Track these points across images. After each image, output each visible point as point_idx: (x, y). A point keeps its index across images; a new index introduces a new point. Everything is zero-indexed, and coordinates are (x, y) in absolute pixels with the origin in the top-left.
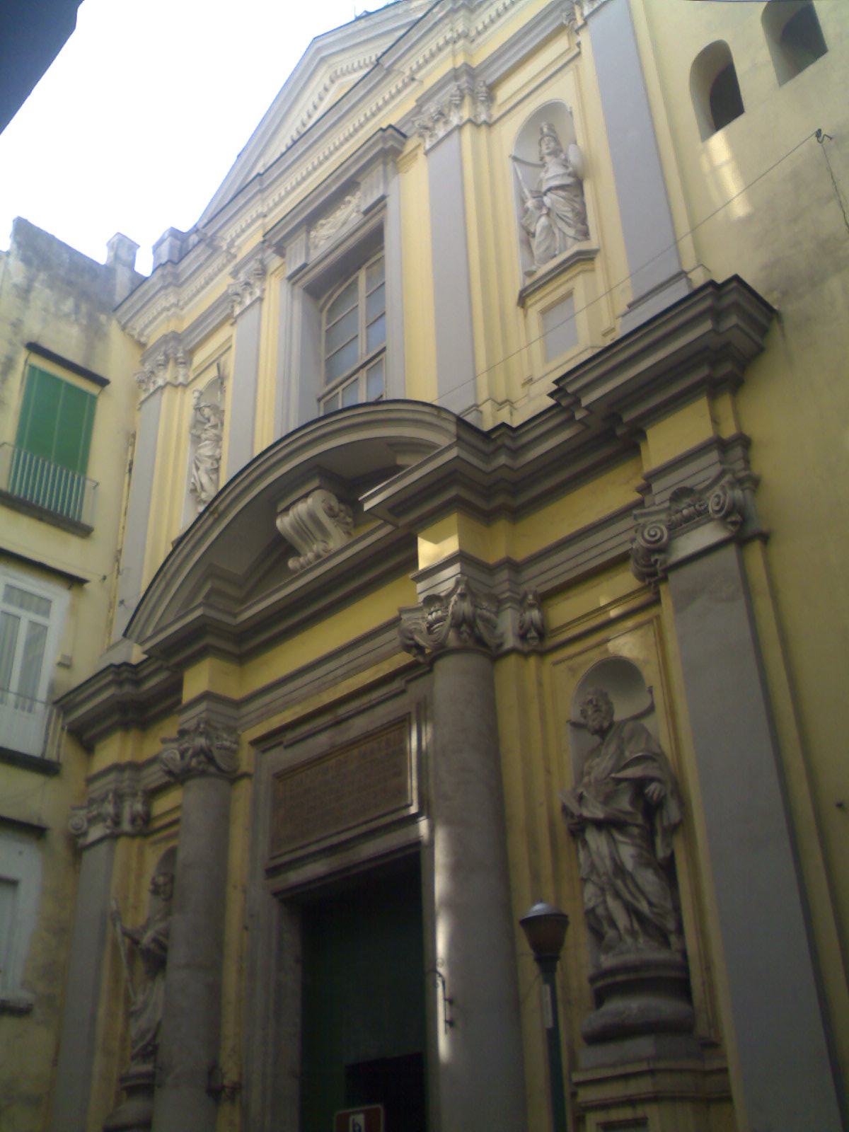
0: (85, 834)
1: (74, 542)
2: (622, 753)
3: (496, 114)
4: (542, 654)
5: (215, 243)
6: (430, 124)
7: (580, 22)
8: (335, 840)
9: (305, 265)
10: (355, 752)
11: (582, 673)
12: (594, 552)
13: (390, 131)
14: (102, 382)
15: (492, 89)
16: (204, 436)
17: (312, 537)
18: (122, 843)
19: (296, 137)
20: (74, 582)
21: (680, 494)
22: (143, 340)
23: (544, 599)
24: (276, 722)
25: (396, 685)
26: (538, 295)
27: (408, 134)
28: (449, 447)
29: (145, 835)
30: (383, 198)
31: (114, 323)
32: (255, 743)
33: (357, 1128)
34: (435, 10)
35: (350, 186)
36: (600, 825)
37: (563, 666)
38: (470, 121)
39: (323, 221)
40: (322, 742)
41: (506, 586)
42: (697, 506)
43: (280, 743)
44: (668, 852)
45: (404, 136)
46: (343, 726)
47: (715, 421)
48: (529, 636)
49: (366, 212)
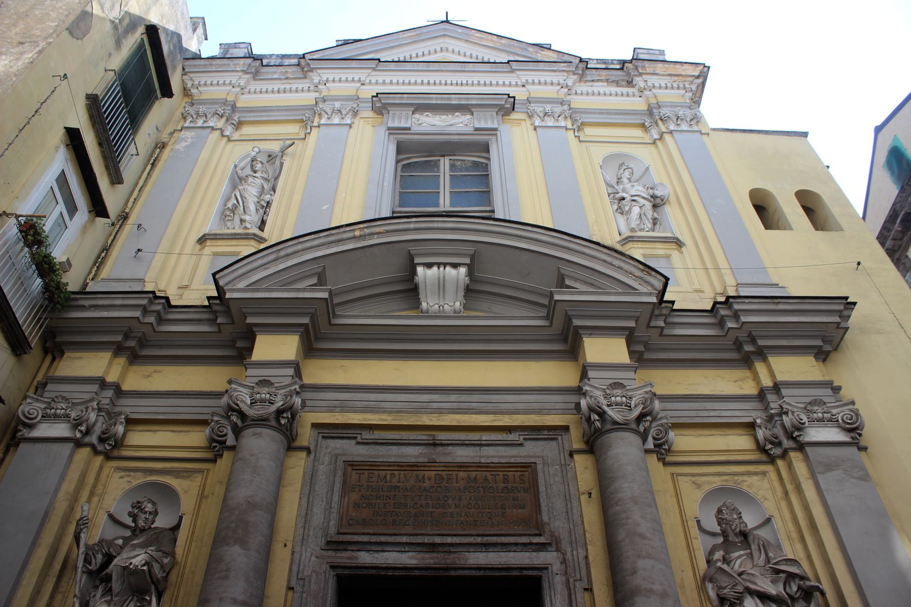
0: (31, 427)
8: (438, 540)
11: (707, 488)
12: (706, 414)
13: (512, 100)
17: (441, 295)
18: (85, 452)
19: (402, 59)
25: (512, 437)
28: (650, 294)
32: (315, 426)
34: (562, 64)
37: (686, 479)
40: (412, 453)
43: (356, 438)
46: (440, 449)
49: (477, 129)
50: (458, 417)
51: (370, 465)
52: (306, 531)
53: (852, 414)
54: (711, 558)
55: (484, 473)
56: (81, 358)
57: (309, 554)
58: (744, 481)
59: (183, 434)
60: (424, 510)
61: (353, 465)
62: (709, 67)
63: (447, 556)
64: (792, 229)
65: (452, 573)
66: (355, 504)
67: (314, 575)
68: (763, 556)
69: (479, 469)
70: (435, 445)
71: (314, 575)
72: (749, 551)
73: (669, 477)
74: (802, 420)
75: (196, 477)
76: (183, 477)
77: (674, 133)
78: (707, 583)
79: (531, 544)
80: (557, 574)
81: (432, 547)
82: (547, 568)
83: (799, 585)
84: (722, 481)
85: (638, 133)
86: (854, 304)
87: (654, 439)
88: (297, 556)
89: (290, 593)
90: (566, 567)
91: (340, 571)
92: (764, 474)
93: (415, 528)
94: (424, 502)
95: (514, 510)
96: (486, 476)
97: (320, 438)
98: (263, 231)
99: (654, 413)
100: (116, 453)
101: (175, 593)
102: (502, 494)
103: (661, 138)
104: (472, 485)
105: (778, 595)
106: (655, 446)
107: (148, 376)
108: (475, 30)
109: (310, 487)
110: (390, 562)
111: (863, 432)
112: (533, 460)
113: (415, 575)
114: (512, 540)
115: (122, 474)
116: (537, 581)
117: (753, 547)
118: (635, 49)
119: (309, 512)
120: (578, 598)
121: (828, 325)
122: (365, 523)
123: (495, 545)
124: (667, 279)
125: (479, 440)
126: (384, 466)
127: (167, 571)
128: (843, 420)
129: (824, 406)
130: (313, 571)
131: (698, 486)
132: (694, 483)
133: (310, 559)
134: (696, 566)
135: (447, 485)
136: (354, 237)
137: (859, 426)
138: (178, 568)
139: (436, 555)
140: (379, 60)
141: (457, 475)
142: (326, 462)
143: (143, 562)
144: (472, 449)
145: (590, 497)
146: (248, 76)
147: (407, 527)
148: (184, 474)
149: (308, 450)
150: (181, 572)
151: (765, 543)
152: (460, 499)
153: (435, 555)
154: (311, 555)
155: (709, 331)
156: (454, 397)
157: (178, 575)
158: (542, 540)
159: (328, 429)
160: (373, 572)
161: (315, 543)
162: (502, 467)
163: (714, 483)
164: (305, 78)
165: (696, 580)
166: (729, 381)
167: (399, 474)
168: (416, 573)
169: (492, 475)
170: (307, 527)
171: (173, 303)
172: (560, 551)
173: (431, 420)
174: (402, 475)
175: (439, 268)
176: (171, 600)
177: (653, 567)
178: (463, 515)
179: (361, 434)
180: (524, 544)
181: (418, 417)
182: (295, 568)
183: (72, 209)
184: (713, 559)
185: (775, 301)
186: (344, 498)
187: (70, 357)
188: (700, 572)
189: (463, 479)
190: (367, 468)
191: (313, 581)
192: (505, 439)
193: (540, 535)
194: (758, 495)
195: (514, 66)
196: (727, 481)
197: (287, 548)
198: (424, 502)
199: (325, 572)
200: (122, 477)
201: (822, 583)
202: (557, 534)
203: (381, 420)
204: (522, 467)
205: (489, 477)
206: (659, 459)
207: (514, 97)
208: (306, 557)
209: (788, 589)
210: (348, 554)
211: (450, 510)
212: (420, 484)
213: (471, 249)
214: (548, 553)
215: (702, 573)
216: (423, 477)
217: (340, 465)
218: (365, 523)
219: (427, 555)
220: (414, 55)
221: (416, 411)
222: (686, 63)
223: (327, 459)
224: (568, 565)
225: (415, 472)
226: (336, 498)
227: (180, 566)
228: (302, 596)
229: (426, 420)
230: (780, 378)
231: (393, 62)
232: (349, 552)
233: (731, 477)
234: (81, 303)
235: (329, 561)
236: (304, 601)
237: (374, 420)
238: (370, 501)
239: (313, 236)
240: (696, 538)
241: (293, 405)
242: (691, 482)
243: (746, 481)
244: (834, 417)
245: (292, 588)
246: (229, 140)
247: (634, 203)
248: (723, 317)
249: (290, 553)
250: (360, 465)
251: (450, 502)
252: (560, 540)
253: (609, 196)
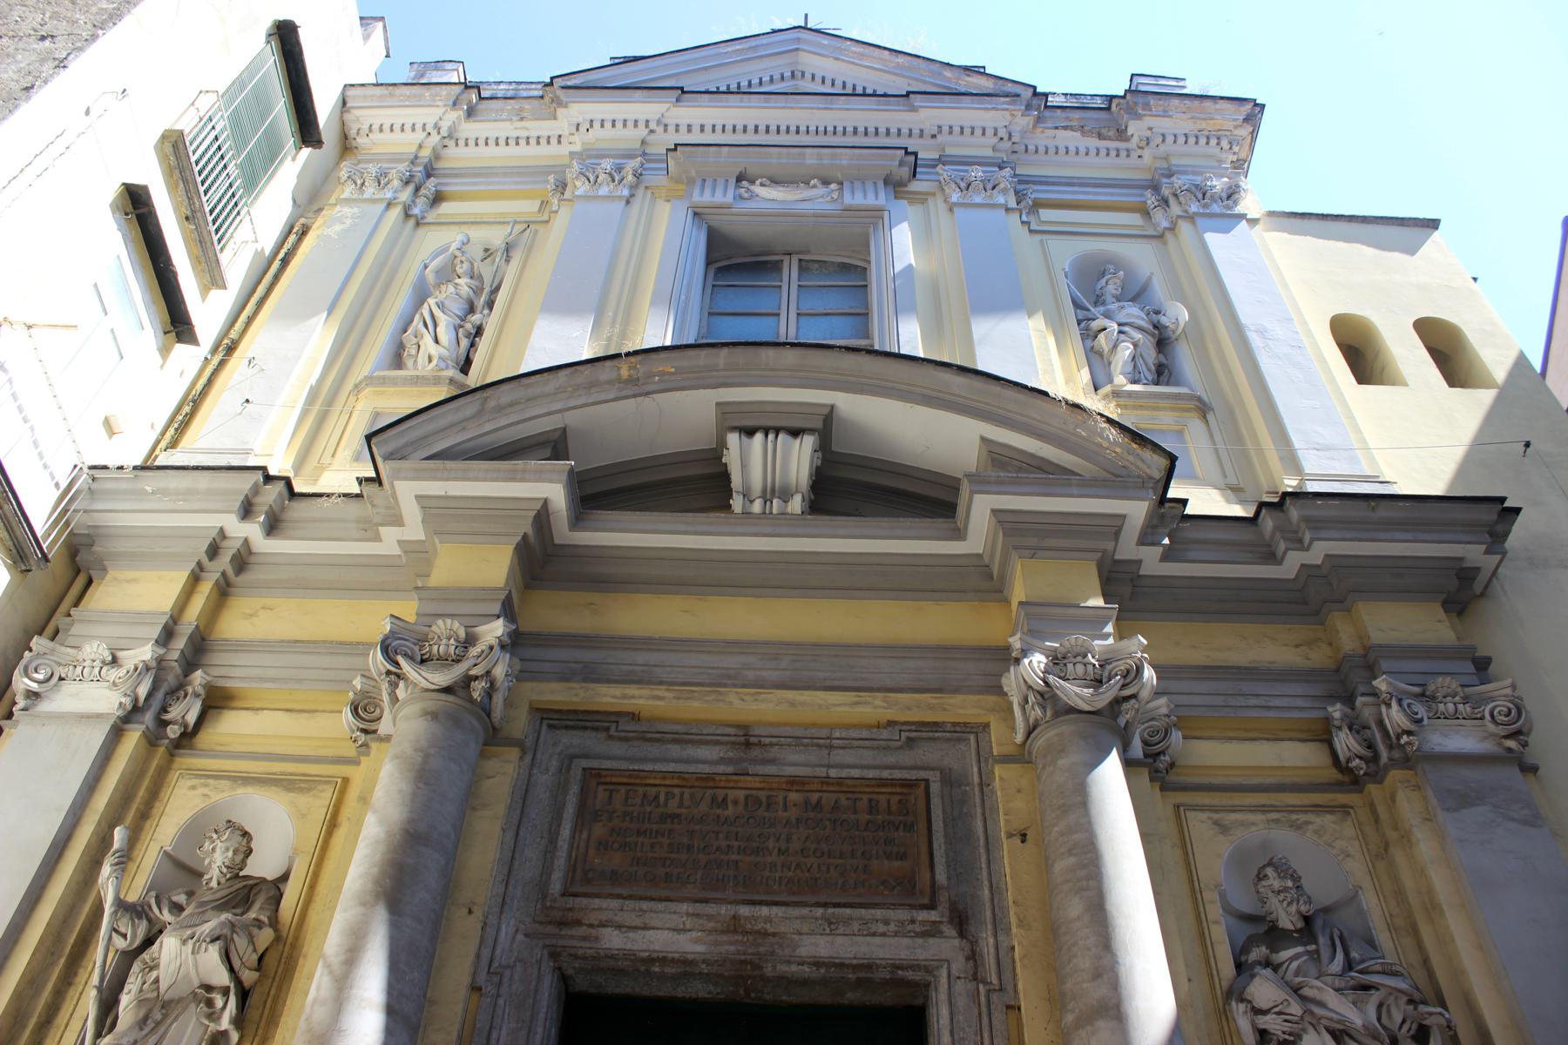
19: (723, 88)
34: (1002, 99)
37: (1203, 816)
52: (510, 888)
53: (1511, 706)
54: (1243, 958)
55: (834, 796)
56: (135, 580)
57: (511, 930)
58: (1308, 823)
59: (306, 715)
60: (723, 857)
62: (1263, 106)
63: (760, 941)
64: (1406, 385)
66: (600, 844)
67: (519, 968)
68: (1340, 956)
69: (825, 788)
71: (519, 968)
72: (1313, 947)
73: (1170, 811)
74: (1417, 714)
75: (322, 791)
76: (301, 790)
77: (1196, 218)
78: (1234, 1003)
80: (959, 978)
83: (1405, 1010)
84: (1268, 821)
85: (1134, 219)
86: (1517, 511)
87: (1145, 743)
88: (491, 932)
89: (475, 996)
90: (976, 967)
92: (1345, 810)
93: (704, 889)
94: (723, 843)
95: (886, 862)
96: (836, 802)
97: (544, 727)
98: (466, 374)
101: (272, 993)
102: (866, 834)
103: (1172, 228)
104: (811, 815)
106: (1146, 755)
107: (251, 615)
108: (851, 40)
109: (522, 812)
110: (657, 948)
111: (1531, 739)
112: (923, 774)
115: (195, 782)
117: (1321, 940)
118: (1133, 75)
119: (517, 855)
120: (995, 1022)
124: (1173, 459)
125: (828, 738)
127: (260, 952)
128: (1492, 715)
131: (1224, 829)
132: (1216, 823)
133: (514, 938)
134: (1215, 973)
137: (1523, 725)
138: (281, 947)
139: (740, 938)
140: (682, 89)
141: (785, 798)
142: (553, 769)
145: (1023, 842)
148: (302, 785)
149: (519, 744)
150: (285, 955)
151: (1345, 934)
152: (788, 840)
154: (517, 931)
157: (280, 960)
162: (868, 786)
163: (1253, 824)
165: (1214, 997)
166: (1286, 645)
167: (682, 794)
169: (848, 799)
170: (512, 881)
171: (298, 488)
173: (743, 700)
174: (687, 796)
175: (766, 436)
176: (265, 1002)
178: (793, 868)
179: (617, 722)
181: (721, 693)
184: (1247, 960)
186: (581, 831)
187: (115, 579)
188: (1222, 983)
189: (795, 805)
191: (516, 977)
192: (874, 736)
194: (1334, 847)
195: (917, 100)
197: (473, 916)
198: (723, 843)
199: (539, 962)
200: (193, 788)
201: (1448, 1003)
202: (961, 907)
204: (902, 786)
205: (844, 802)
206: (1152, 780)
207: (916, 154)
208: (507, 934)
209: (1384, 1020)
211: (769, 859)
212: (717, 811)
214: (943, 940)
215: (1225, 984)
217: (576, 774)
220: (744, 84)
222: (1222, 98)
223: (555, 763)
224: (979, 963)
225: (710, 791)
226: (566, 832)
227: (285, 944)
228: (495, 1004)
230: (1377, 637)
231: (707, 92)
232: (585, 928)
233: (1285, 814)
235: (548, 942)
236: (499, 1012)
238: (628, 840)
240: (1216, 922)
242: (1210, 822)
244: (1476, 711)
246: (418, 224)
247: (1122, 337)
249: (479, 926)
251: (771, 844)
252: (967, 917)
253: (1079, 324)
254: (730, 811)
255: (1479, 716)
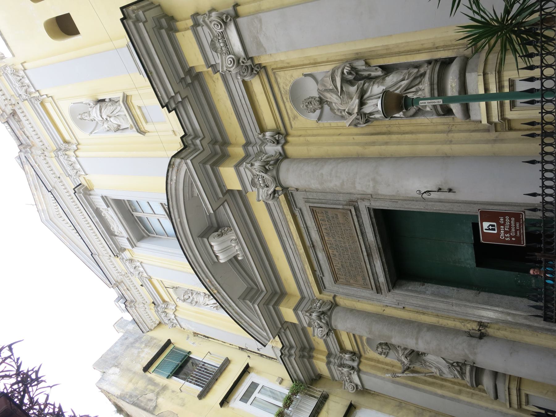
0: (357, 385)
1: (231, 367)
2: (330, 90)
3: (74, 141)
4: (287, 134)
5: (119, 281)
6: (75, 171)
7: (37, 94)
8: (365, 254)
9: (128, 239)
10: (326, 238)
11: (295, 112)
13: (76, 189)
14: (169, 343)
15: (66, 142)
16: (195, 300)
17: (230, 247)
20: (247, 370)
21: (213, 46)
22: (157, 323)
23: (263, 130)
24: (311, 279)
25: (297, 213)
26: (140, 124)
27: (80, 183)
28: (186, 164)
29: (360, 357)
30: (102, 197)
31: (148, 333)
32: (320, 292)
33: (491, 227)
35: (98, 212)
36: (362, 104)
37: (293, 123)
38: (74, 152)
39: (111, 228)
40: (321, 256)
41: (255, 148)
42: (219, 38)
44: (379, 69)
45: (80, 184)
46: (315, 244)
47: (186, 29)
48: (277, 139)
49: (108, 206)
50: (295, 238)
51: (334, 274)
56: (319, 369)
58: (283, 88)
61: (336, 281)
65: (381, 246)
70: (313, 246)
79: (356, 215)
81: (369, 255)
82: (368, 208)
91: (391, 288)
97: (326, 290)
99: (263, 164)
100: (358, 353)
105: (358, 98)
113: (385, 260)
114: (357, 224)
116: (375, 210)
121: (148, 31)
122: (364, 279)
123: (361, 230)
126: (332, 269)
129: (213, 40)
130: (394, 298)
132: (294, 119)
135: (334, 245)
136: (218, 292)
143: (405, 359)
144: (310, 231)
146: (137, 305)
147: (362, 264)
153: (373, 254)
155: (188, 107)
156: (285, 239)
158: (353, 210)
159: (320, 287)
160: (388, 276)
161: (379, 296)
164: (122, 282)
168: (384, 260)
172: (357, 200)
177: (359, 183)
180: (357, 217)
182: (394, 306)
183: (254, 386)
185: (150, 75)
190: (335, 275)
191: (398, 299)
193: (350, 211)
194: (290, 81)
196: (287, 99)
203: (308, 269)
207: (74, 189)
210: (381, 286)
213: (198, 240)
216: (333, 254)
218: (364, 279)
219: (374, 257)
221: (299, 255)
229: (302, 251)
233: (283, 95)
234: (296, 377)
237: (310, 273)
239: (226, 309)
241: (317, 316)
243: (283, 86)
244: (220, 35)
245: (404, 308)
248: (176, 104)
250: (335, 278)
254: (335, 253)
255: (222, 33)
